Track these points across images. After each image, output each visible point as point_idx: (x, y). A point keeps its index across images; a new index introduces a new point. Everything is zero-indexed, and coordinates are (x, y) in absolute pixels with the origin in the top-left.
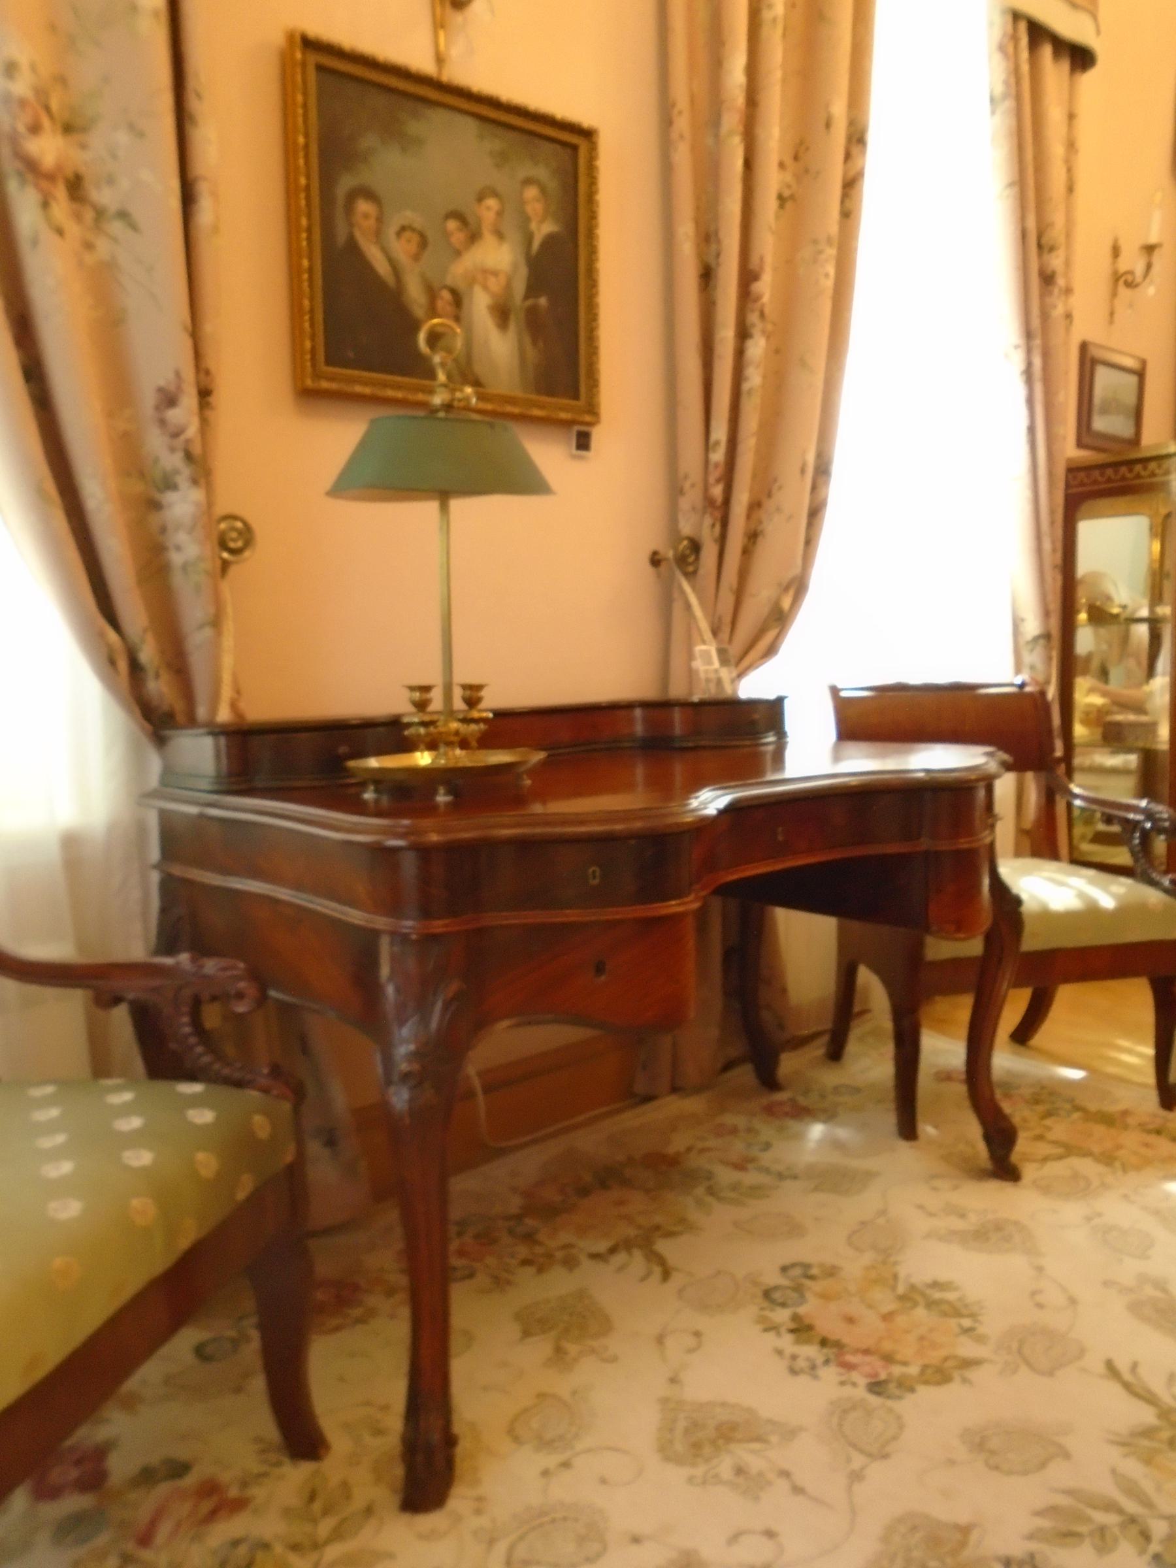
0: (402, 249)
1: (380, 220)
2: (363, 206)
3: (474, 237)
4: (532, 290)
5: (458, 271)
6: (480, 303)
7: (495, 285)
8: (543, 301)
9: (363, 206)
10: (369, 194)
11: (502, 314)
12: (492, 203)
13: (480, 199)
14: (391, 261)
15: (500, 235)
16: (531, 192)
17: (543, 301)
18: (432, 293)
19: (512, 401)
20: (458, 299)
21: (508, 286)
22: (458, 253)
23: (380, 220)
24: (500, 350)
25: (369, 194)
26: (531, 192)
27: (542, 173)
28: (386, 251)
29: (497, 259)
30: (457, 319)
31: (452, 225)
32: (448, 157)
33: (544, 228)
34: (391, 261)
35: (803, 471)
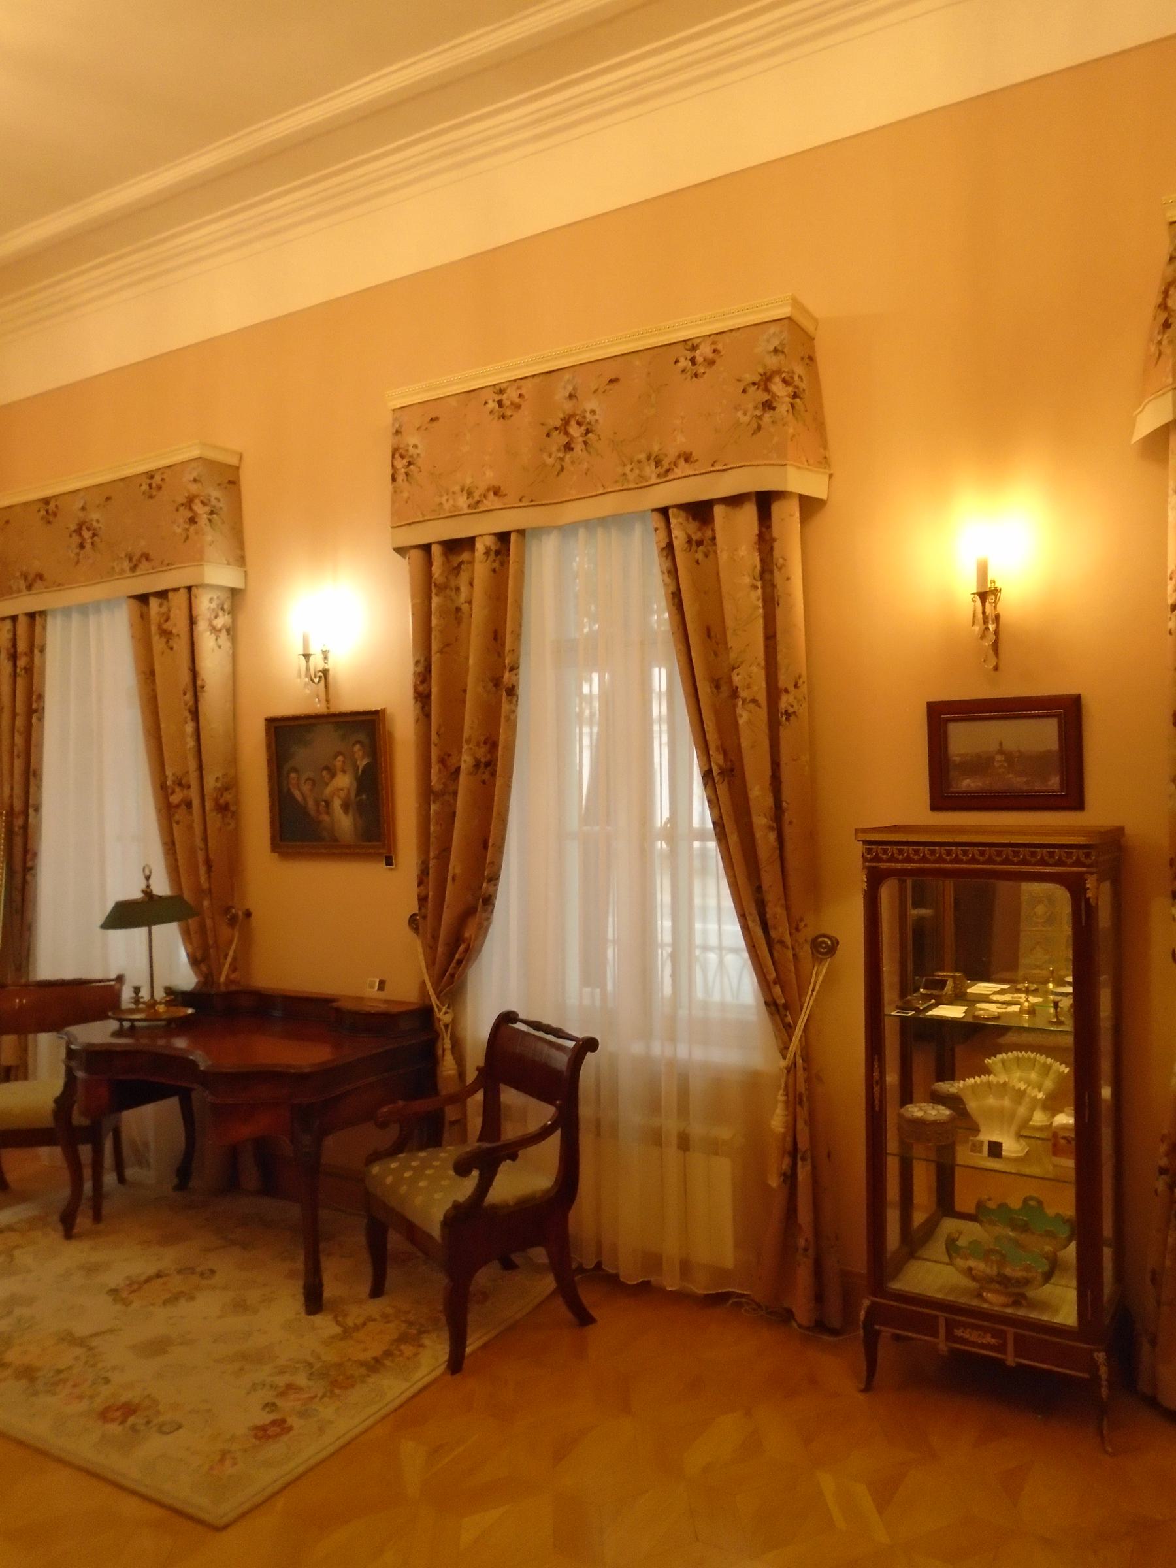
0: (306, 788)
1: (298, 779)
2: (293, 775)
3: (333, 775)
4: (358, 793)
5: (328, 791)
6: (337, 804)
7: (343, 794)
8: (364, 797)
9: (293, 775)
10: (294, 770)
11: (346, 807)
12: (340, 758)
13: (335, 757)
14: (302, 794)
15: (344, 771)
16: (357, 747)
17: (364, 797)
18: (317, 804)
19: (349, 847)
20: (328, 804)
21: (349, 793)
22: (327, 784)
23: (298, 779)
24: (344, 823)
25: (294, 770)
26: (357, 747)
27: (362, 737)
28: (302, 791)
29: (344, 781)
30: (328, 813)
31: (324, 773)
32: (325, 743)
33: (363, 763)
34: (302, 794)
35: (454, 879)
